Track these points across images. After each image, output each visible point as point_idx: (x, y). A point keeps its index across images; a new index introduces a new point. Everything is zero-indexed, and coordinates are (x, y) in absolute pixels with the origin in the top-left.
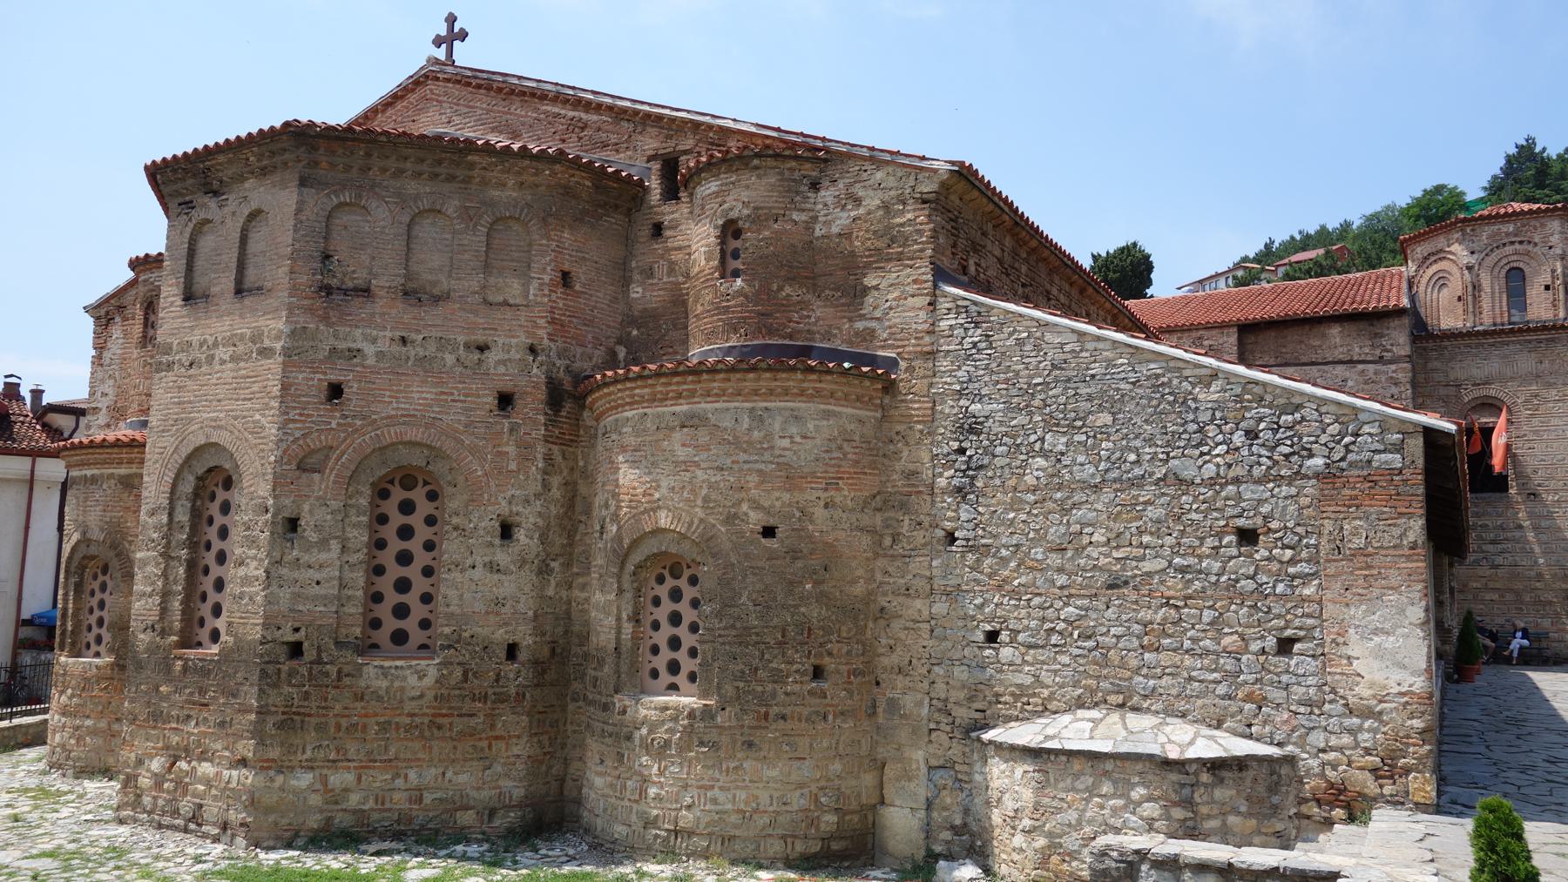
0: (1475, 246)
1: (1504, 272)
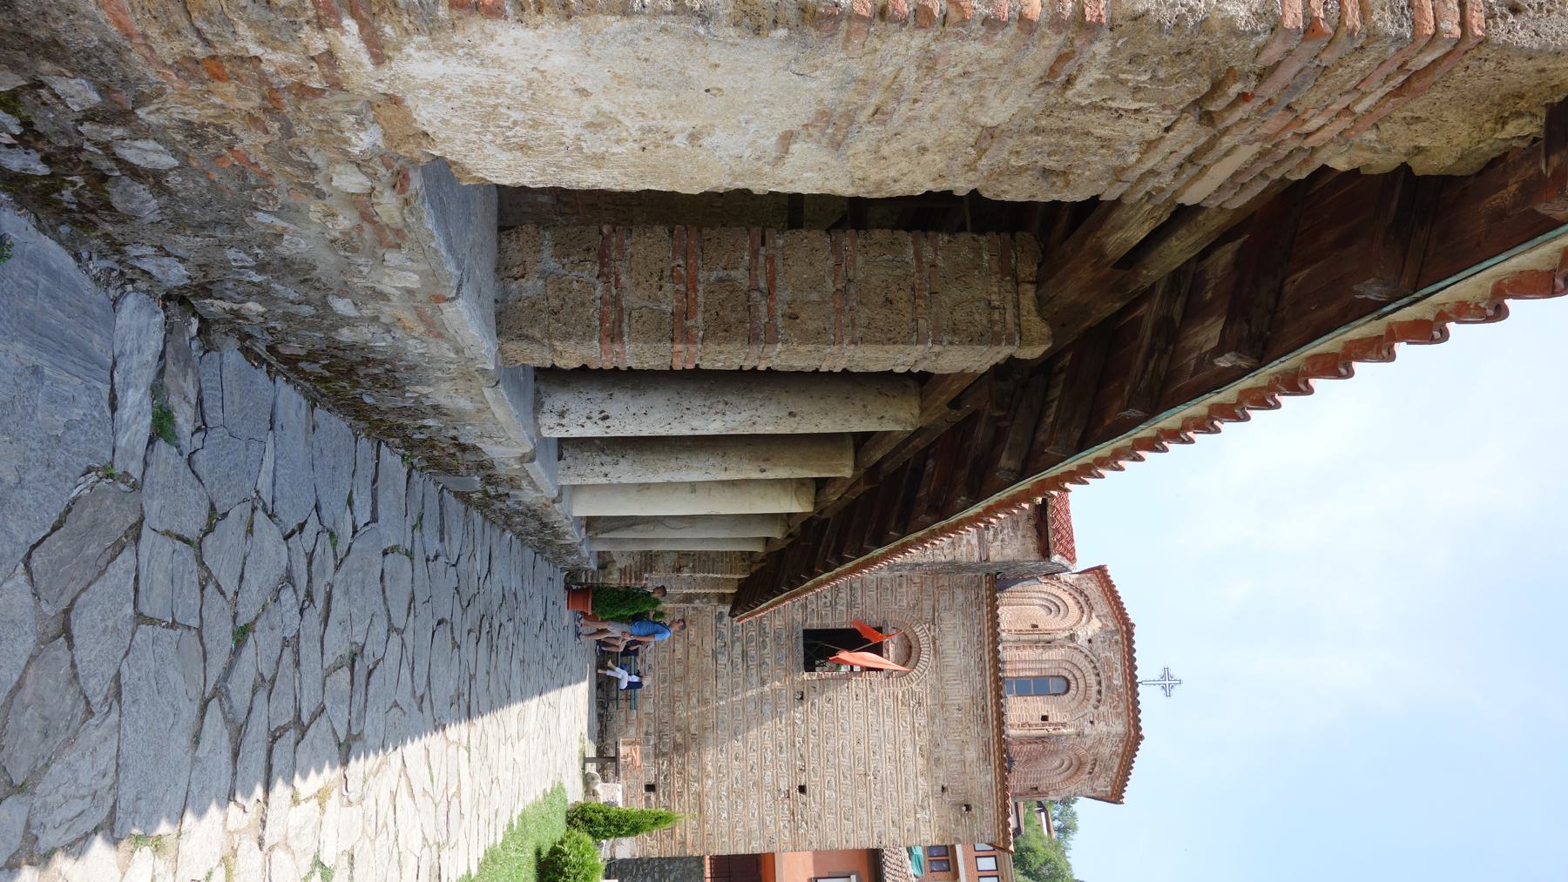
0: (1097, 644)
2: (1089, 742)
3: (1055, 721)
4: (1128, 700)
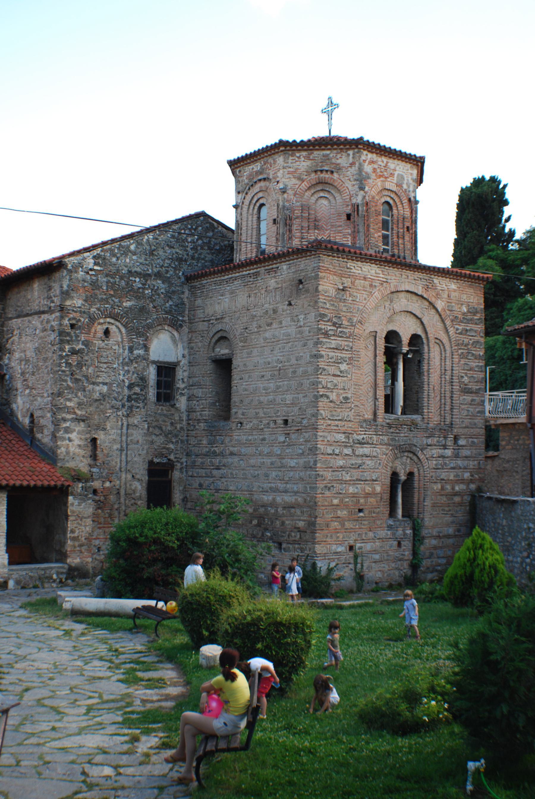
1: (256, 208)
2: (294, 181)
3: (276, 213)
4: (266, 156)
